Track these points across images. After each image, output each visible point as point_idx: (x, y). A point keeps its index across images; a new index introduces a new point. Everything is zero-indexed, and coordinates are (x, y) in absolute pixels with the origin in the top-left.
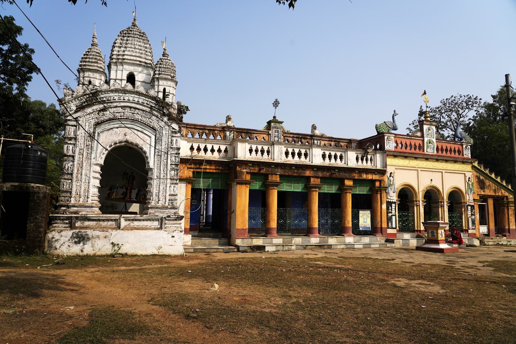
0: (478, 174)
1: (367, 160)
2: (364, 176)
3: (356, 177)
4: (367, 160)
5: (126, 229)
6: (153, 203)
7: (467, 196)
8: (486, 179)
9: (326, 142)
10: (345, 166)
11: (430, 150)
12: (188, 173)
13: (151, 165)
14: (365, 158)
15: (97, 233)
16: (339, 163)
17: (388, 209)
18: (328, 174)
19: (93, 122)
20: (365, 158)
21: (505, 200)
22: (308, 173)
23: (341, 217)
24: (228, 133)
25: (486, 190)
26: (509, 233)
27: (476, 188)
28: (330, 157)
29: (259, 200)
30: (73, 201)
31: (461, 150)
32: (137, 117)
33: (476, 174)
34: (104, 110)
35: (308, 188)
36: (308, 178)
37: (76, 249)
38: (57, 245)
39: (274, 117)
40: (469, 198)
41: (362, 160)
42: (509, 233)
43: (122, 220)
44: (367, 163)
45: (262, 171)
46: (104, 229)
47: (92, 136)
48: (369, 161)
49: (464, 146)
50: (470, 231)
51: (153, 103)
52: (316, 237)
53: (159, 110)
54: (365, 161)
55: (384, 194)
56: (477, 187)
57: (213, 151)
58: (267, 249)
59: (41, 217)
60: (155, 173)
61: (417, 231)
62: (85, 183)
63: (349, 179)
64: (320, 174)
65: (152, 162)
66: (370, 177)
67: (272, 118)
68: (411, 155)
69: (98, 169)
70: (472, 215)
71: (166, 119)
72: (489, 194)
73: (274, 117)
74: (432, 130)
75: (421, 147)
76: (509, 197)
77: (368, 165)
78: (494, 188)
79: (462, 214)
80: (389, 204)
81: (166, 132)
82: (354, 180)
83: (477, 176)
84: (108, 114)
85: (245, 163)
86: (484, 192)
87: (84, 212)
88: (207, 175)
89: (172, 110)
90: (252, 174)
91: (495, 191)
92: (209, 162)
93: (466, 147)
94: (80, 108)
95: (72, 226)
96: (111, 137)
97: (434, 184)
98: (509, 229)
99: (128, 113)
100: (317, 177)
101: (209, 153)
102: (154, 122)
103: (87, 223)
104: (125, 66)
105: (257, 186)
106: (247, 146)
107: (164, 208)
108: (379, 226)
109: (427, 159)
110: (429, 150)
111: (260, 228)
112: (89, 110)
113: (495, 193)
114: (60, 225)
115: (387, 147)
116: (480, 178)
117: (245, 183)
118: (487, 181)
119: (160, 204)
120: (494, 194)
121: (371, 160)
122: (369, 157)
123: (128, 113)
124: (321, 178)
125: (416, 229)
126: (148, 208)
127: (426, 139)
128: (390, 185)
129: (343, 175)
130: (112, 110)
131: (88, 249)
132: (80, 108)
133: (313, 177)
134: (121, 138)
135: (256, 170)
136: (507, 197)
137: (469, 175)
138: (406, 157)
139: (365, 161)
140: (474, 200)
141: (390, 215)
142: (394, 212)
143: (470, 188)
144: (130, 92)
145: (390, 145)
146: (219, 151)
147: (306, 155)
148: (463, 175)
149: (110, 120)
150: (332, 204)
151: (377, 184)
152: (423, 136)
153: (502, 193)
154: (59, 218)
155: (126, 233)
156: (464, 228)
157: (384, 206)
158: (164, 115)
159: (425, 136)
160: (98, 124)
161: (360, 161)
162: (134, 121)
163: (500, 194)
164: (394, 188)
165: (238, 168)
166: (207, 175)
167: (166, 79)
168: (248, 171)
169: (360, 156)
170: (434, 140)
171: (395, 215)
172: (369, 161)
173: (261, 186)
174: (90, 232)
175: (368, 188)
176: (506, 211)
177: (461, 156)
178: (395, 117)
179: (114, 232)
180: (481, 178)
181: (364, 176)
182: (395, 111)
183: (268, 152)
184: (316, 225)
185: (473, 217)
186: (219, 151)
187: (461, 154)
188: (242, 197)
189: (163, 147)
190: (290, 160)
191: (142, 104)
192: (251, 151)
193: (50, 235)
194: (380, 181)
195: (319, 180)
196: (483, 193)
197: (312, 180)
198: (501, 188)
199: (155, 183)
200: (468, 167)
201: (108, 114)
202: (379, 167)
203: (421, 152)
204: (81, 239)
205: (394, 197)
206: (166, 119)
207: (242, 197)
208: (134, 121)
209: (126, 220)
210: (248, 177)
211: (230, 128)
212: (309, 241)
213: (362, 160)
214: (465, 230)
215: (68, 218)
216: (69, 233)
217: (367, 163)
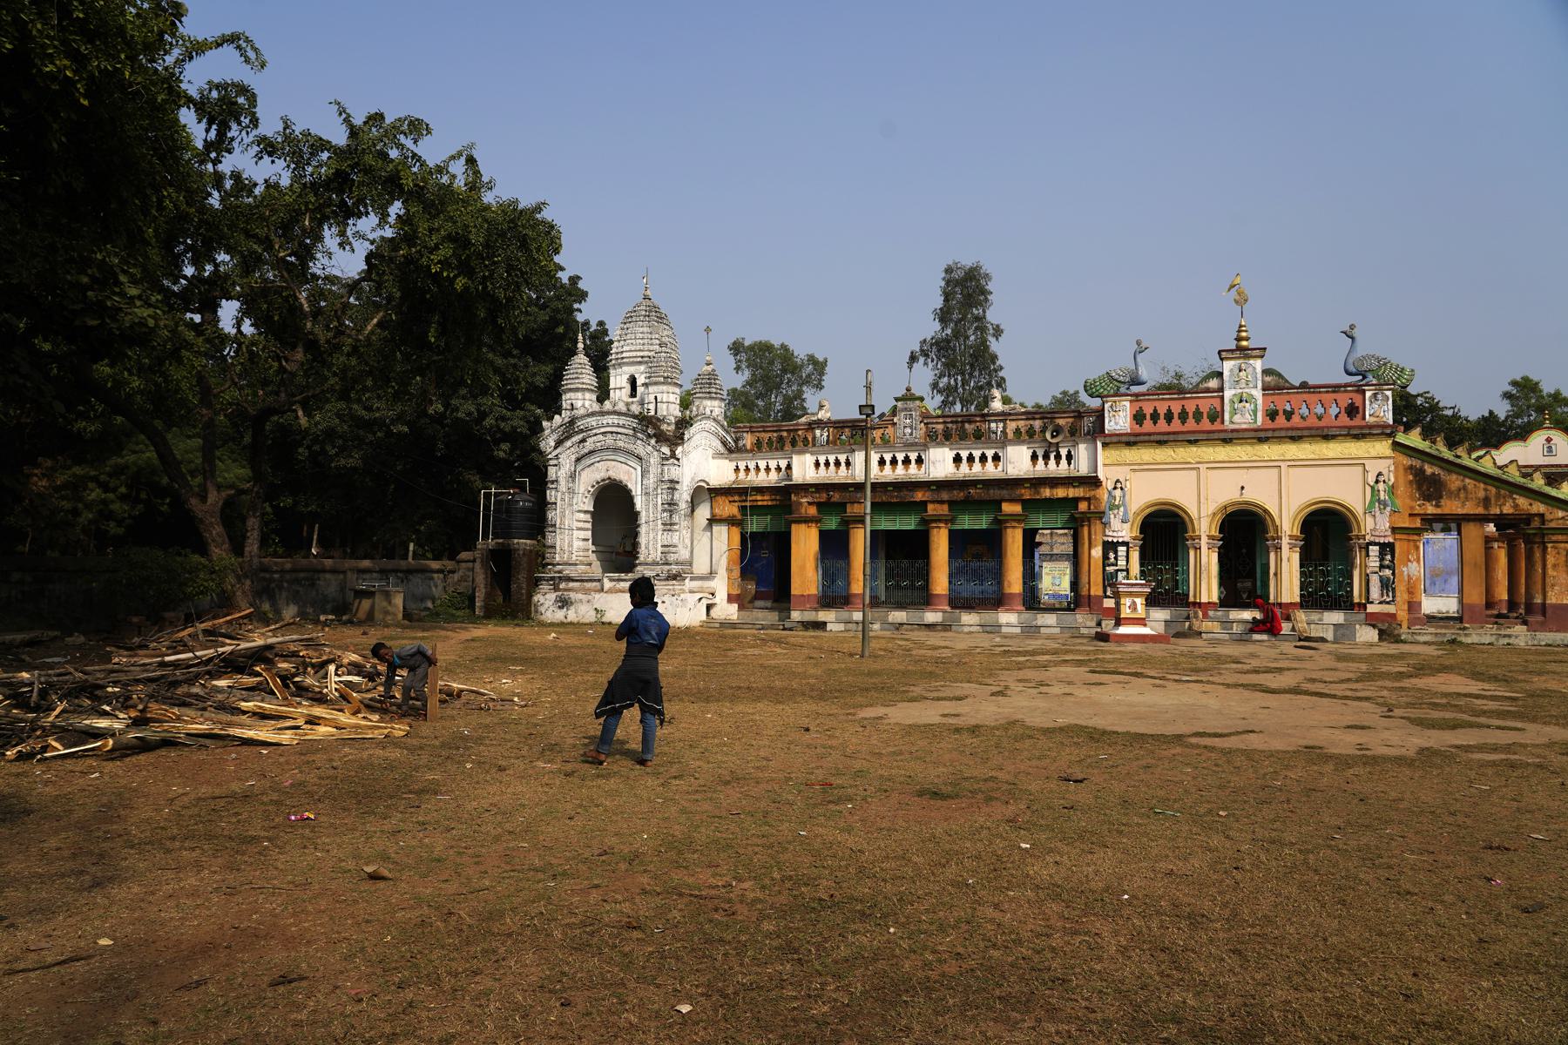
0: (1417, 463)
1: (1058, 457)
2: (1047, 493)
3: (1027, 494)
4: (1058, 457)
5: (610, 591)
6: (642, 558)
7: (1369, 520)
8: (1450, 472)
9: (1021, 423)
10: (1002, 476)
11: (1241, 419)
12: (729, 508)
13: (638, 507)
14: (1052, 456)
15: (580, 596)
16: (991, 471)
17: (1105, 557)
18: (959, 495)
19: (573, 458)
20: (1052, 456)
21: (1536, 523)
22: (919, 496)
23: (998, 575)
24: (818, 432)
25: (1443, 502)
26: (1544, 614)
27: (1409, 502)
28: (971, 459)
29: (834, 547)
30: (558, 559)
31: (1358, 403)
32: (621, 444)
33: (1407, 461)
34: (583, 441)
35: (927, 524)
36: (924, 504)
37: (559, 615)
38: (542, 609)
39: (908, 390)
40: (1374, 525)
41: (1046, 457)
42: (1544, 614)
43: (606, 580)
44: (1058, 464)
45: (834, 499)
46: (587, 591)
47: (573, 476)
48: (1064, 461)
49: (1368, 394)
50: (1371, 609)
51: (634, 423)
52: (935, 611)
53: (643, 432)
54: (1052, 461)
55: (1097, 527)
56: (1412, 498)
57: (768, 469)
58: (829, 627)
59: (522, 577)
60: (643, 518)
61: (1194, 604)
62: (572, 534)
63: (1011, 501)
64: (945, 496)
65: (639, 504)
66: (1061, 493)
67: (901, 392)
68: (1171, 437)
69: (588, 517)
70: (1382, 567)
71: (653, 441)
72: (1460, 511)
73: (908, 390)
74: (1250, 370)
75: (1216, 416)
76: (1548, 516)
77: (1063, 469)
78: (1481, 494)
79: (1352, 565)
80: (1110, 547)
81: (654, 460)
82: (1026, 504)
83: (1411, 467)
84: (589, 445)
85: (804, 488)
86: (1437, 506)
87: (568, 571)
88: (756, 510)
89: (664, 427)
90: (819, 505)
91: (1486, 502)
92: (760, 490)
93: (1375, 395)
94: (559, 443)
95: (556, 589)
96: (591, 477)
97: (1251, 495)
98: (1544, 604)
99: (609, 440)
100: (942, 502)
101: (762, 473)
102: (640, 448)
103: (571, 584)
104: (625, 368)
105: (832, 523)
106: (809, 459)
107: (655, 563)
108: (1084, 592)
109: (1227, 441)
110: (1237, 418)
111: (835, 597)
112: (569, 443)
113: (1486, 507)
114: (545, 587)
115: (1110, 426)
116: (1422, 471)
117: (807, 520)
118: (1454, 477)
119: (650, 560)
120: (1480, 510)
121: (1069, 457)
122: (1064, 452)
123: (609, 440)
124: (951, 503)
125: (1191, 599)
126: (635, 566)
127: (1228, 394)
128: (1113, 507)
129: (995, 493)
130: (590, 440)
131: (572, 615)
132: (559, 443)
133: (933, 502)
134: (599, 476)
135: (823, 497)
136: (1542, 516)
137: (1374, 468)
138: (1160, 443)
139: (1052, 461)
140: (1394, 530)
141: (1110, 569)
142: (1122, 563)
143: (1379, 501)
144: (609, 413)
145: (1119, 419)
146: (779, 469)
147: (920, 461)
148: (1360, 468)
149: (591, 452)
150: (980, 551)
151: (1083, 506)
152: (1221, 389)
153: (1516, 506)
154: (541, 579)
155: (610, 597)
156: (1356, 600)
157: (1097, 552)
158: (649, 436)
159: (1226, 385)
160: (578, 460)
161: (1041, 461)
162: (616, 450)
163: (1507, 509)
164: (1126, 512)
165: (793, 497)
166: (756, 510)
167: (656, 383)
168: (810, 499)
169: (1040, 453)
170: (1258, 394)
171: (1127, 570)
172: (1064, 461)
173: (840, 524)
174: (572, 595)
175: (1066, 516)
176: (1538, 555)
177: (1357, 422)
178: (1139, 357)
179: (597, 596)
180: (1429, 470)
181: (1047, 493)
182: (1138, 343)
183: (848, 463)
184: (857, 587)
185: (1388, 572)
186: (779, 469)
187: (1359, 416)
188: (805, 544)
189: (651, 480)
190: (888, 474)
191: (623, 426)
192: (817, 464)
193: (535, 598)
194: (1088, 499)
195: (946, 507)
196: (1430, 509)
197: (930, 507)
198: (1512, 493)
199: (643, 530)
200: (1383, 447)
201: (589, 445)
202: (1082, 467)
203: (1217, 426)
204: (564, 603)
205: (1123, 529)
206: (653, 441)
207: (805, 544)
208: (616, 450)
209: (611, 580)
210: (813, 511)
211: (820, 424)
212: (922, 618)
213: (1046, 457)
214: (1359, 604)
215: (552, 579)
216: (552, 596)
217: (1058, 464)
